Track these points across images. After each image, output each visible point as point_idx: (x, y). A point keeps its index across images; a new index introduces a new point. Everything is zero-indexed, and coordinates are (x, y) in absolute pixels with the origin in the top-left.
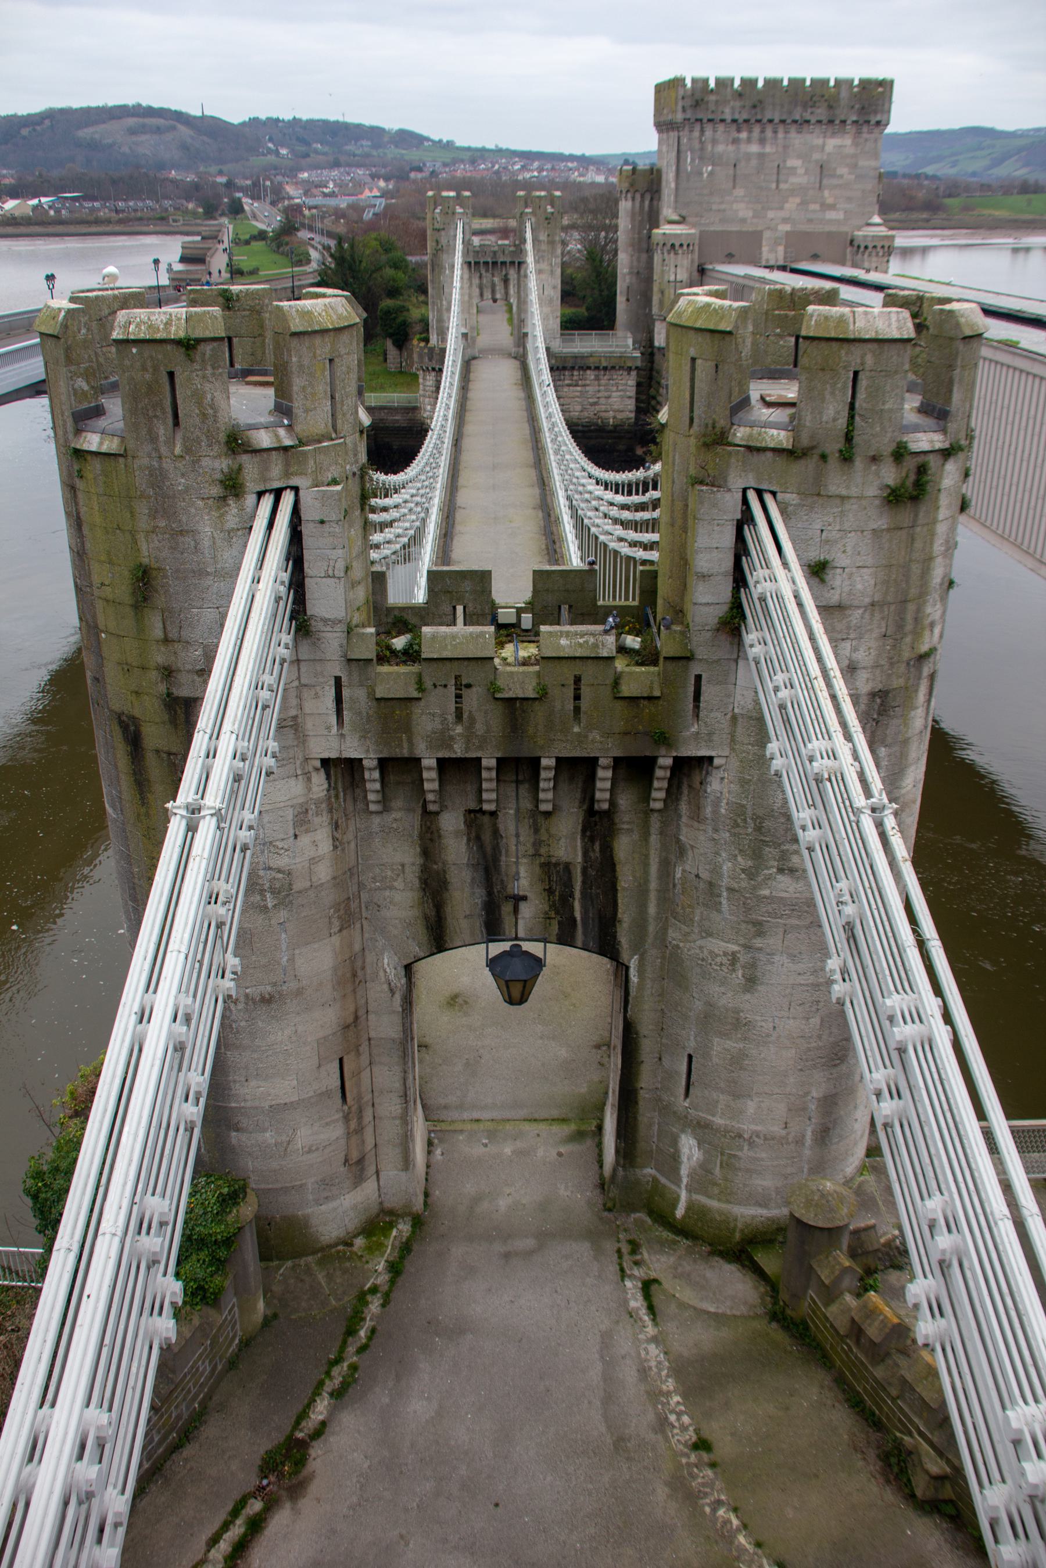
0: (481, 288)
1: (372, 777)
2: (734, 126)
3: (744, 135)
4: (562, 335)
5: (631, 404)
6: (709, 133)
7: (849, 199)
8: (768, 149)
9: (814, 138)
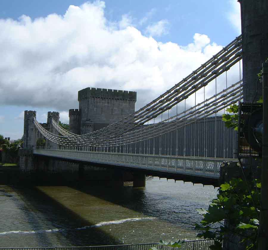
2: (101, 99)
3: (104, 101)
6: (95, 100)
8: (110, 105)
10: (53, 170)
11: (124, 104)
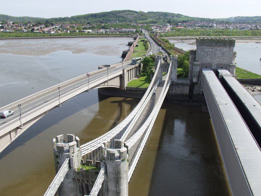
0: (163, 70)
1: (76, 180)
3: (209, 48)
4: (178, 79)
5: (188, 91)
6: (203, 47)
7: (228, 58)
8: (213, 50)
9: (221, 48)
10: (172, 93)
11: (225, 49)
